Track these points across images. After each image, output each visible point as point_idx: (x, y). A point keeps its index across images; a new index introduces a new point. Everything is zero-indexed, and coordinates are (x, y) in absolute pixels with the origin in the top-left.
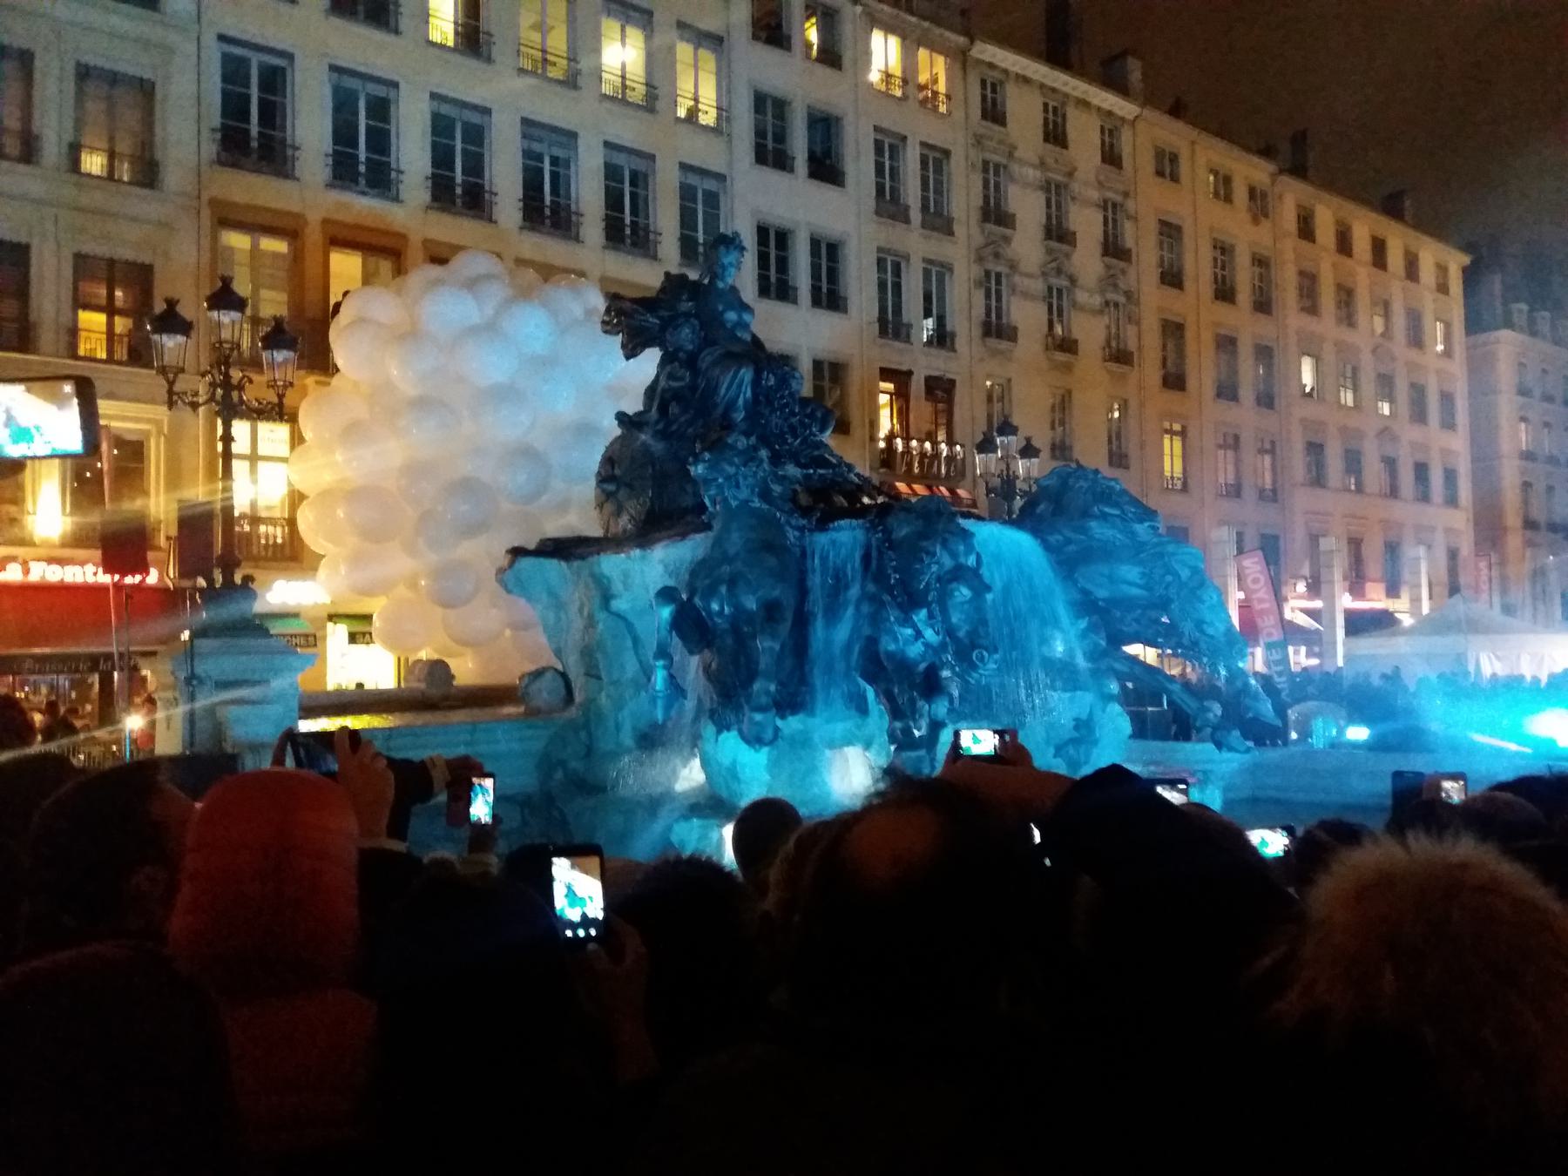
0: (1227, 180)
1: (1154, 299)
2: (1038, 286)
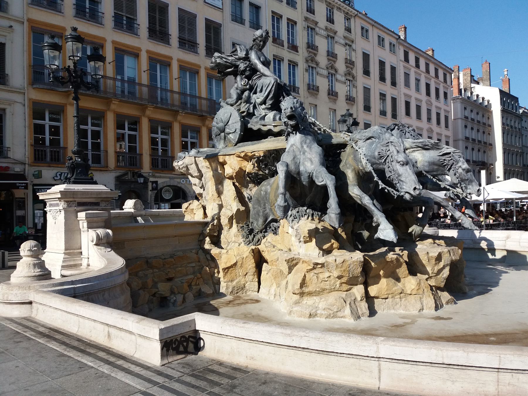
0: (383, 40)
1: (361, 80)
2: (325, 72)
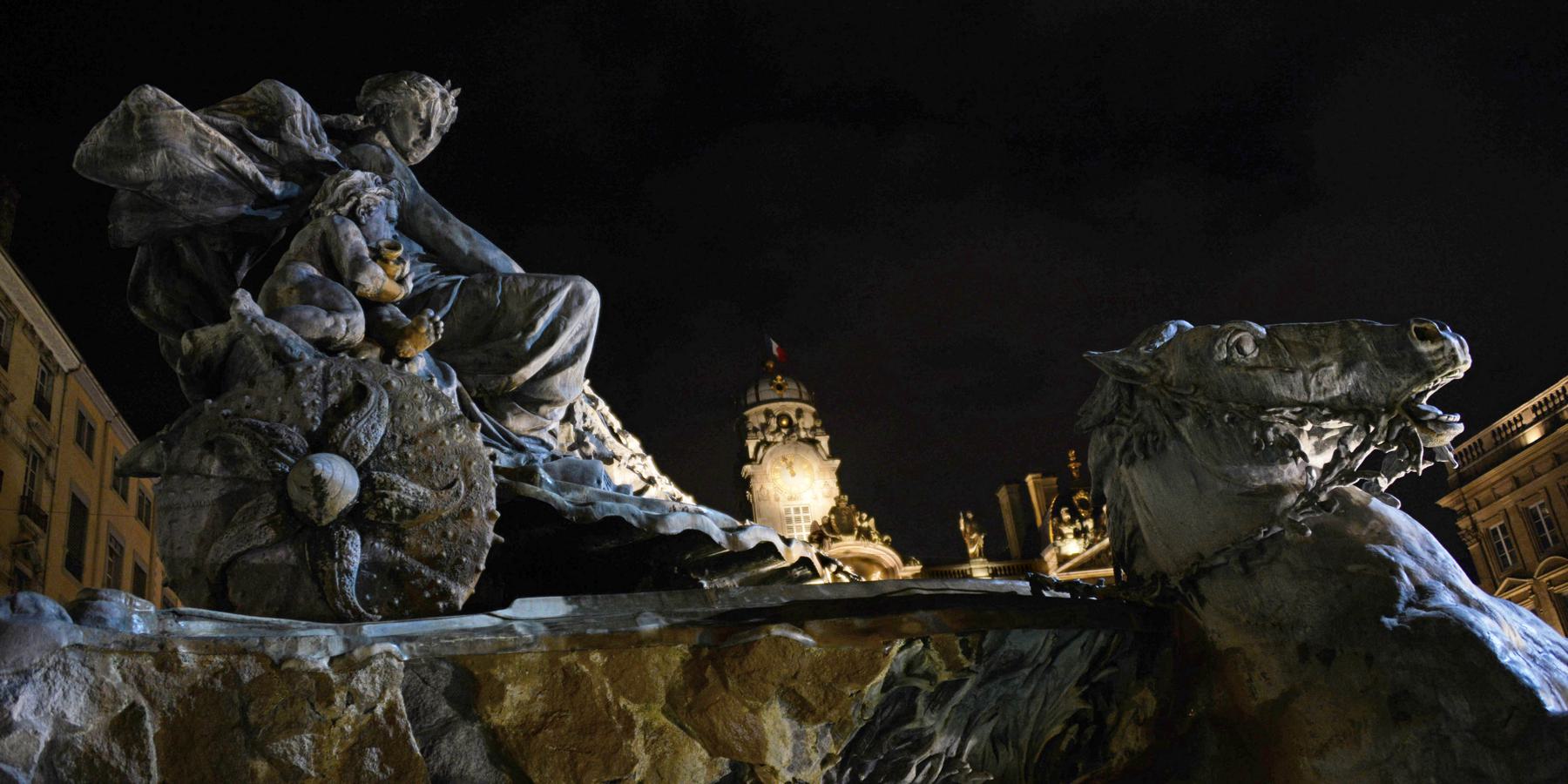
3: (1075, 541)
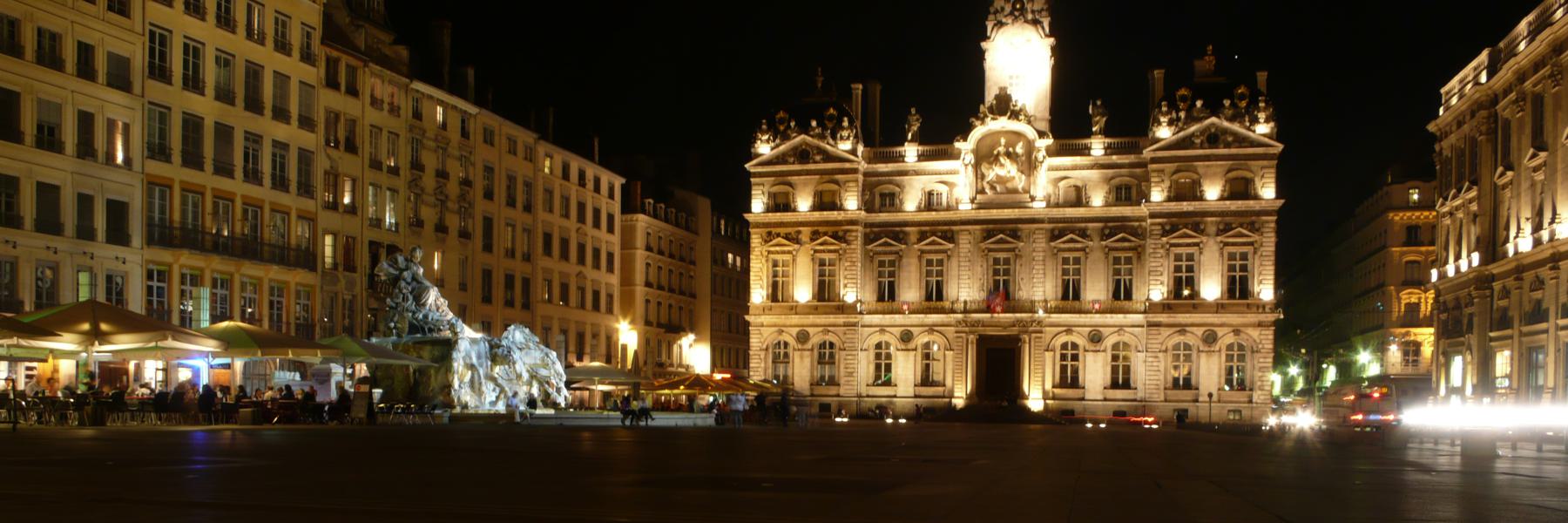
1: (481, 206)
3: (1167, 128)
